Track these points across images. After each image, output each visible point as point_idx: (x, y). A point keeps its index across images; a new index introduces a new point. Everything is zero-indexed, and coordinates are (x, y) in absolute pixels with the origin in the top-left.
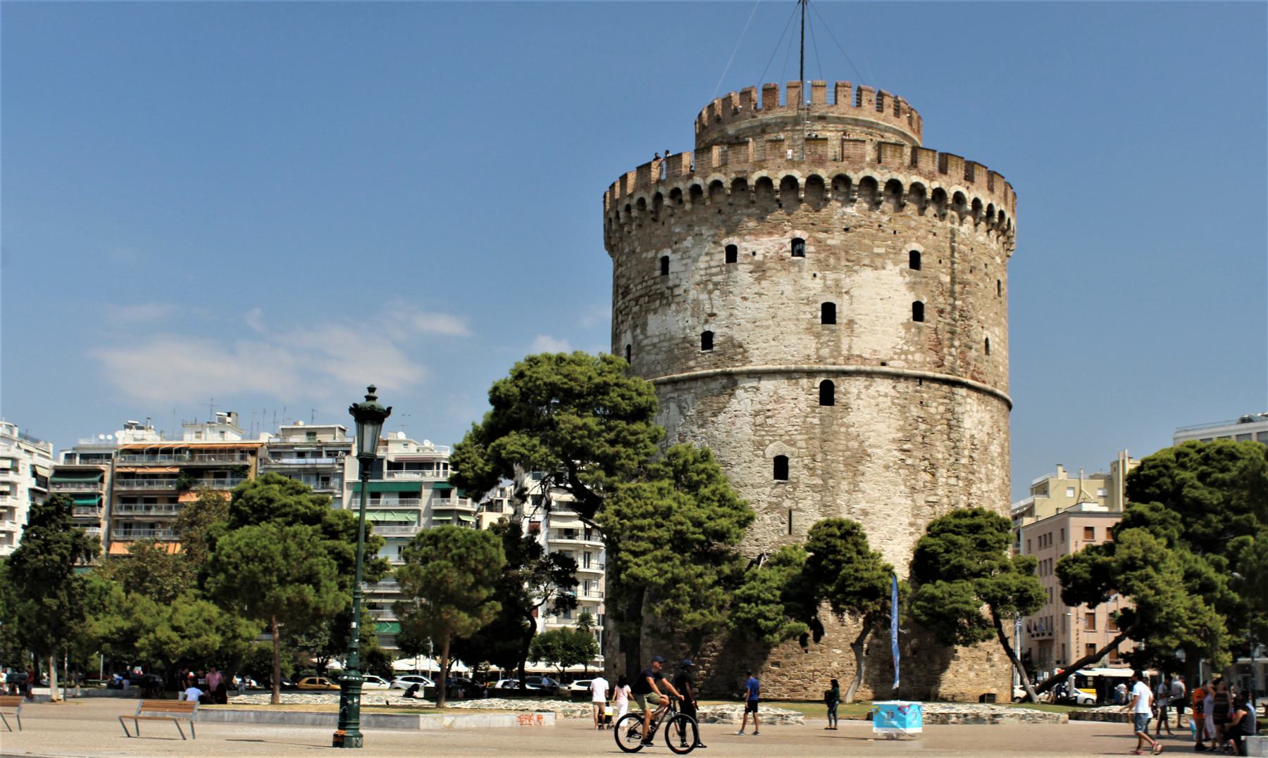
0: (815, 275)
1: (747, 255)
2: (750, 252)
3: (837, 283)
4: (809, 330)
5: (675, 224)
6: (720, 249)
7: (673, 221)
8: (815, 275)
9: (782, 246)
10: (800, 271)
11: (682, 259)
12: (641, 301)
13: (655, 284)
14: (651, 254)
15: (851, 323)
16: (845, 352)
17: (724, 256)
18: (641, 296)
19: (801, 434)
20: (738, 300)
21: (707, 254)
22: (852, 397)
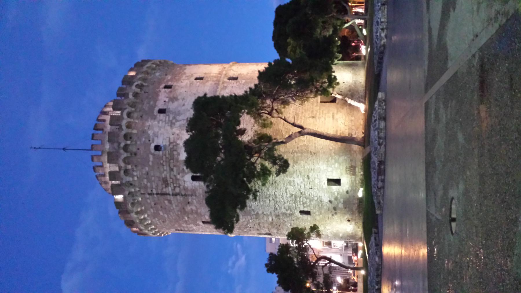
0: (181, 82)
1: (165, 104)
2: (163, 103)
3: (186, 77)
4: (204, 84)
5: (140, 141)
6: (158, 116)
7: (138, 143)
8: (181, 82)
9: (165, 92)
10: (179, 86)
11: (157, 137)
12: (172, 166)
13: (165, 155)
14: (151, 158)
15: (205, 74)
16: (217, 75)
17: (162, 115)
18: (169, 166)
19: (248, 85)
20: (183, 108)
21: (159, 122)
22: (235, 73)
